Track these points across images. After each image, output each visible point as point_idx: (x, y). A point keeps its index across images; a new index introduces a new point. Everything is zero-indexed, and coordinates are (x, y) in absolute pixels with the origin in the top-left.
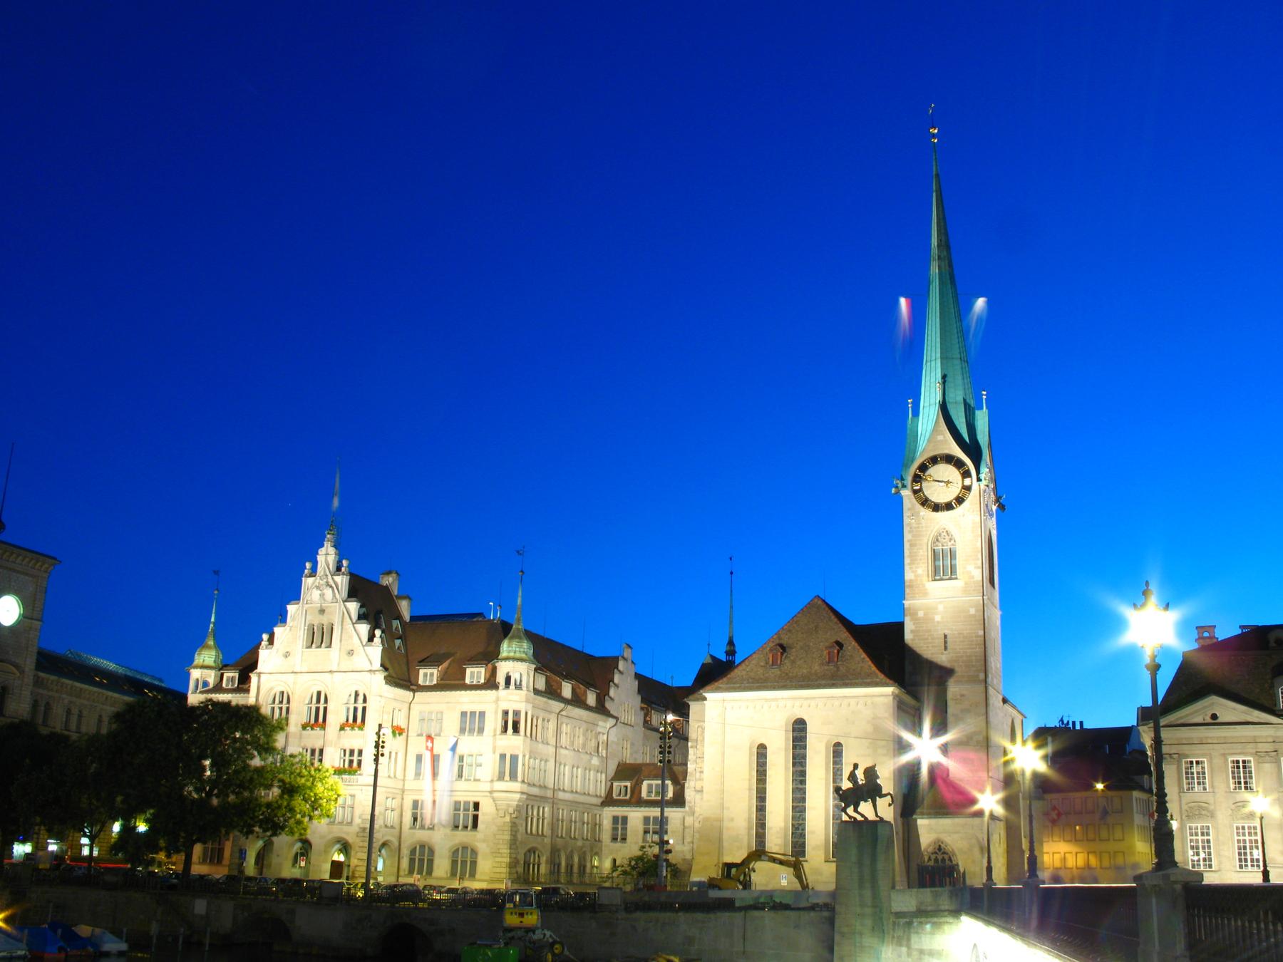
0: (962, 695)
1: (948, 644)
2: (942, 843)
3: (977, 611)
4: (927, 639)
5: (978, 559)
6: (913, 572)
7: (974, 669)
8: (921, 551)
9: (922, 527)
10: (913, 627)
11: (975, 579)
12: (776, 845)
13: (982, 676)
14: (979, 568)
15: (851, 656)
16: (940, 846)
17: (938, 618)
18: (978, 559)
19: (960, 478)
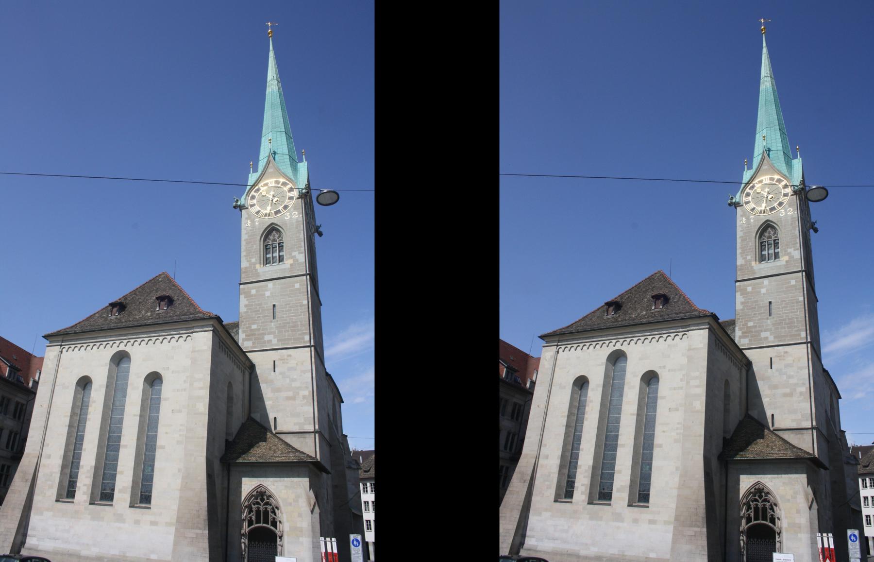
0: (786, 352)
4: (755, 308)
5: (797, 243)
7: (796, 329)
8: (750, 243)
9: (751, 226)
11: (795, 258)
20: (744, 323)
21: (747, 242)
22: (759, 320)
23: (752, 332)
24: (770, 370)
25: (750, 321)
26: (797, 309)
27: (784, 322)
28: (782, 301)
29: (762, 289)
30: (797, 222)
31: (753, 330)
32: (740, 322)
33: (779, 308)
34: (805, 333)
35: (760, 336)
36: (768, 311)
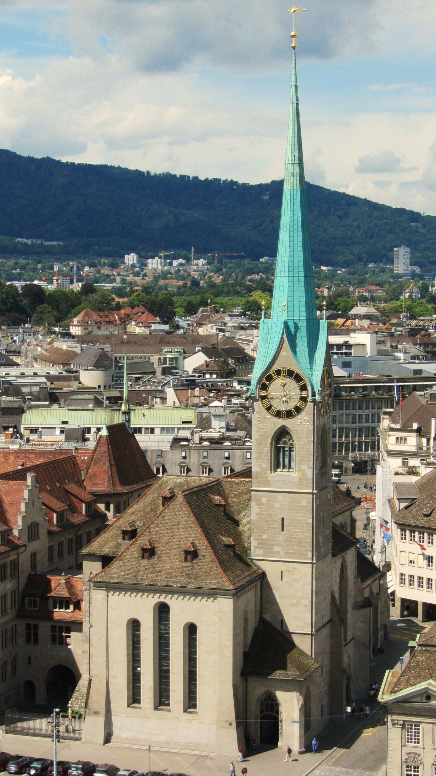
0: (294, 568)
1: (285, 527)
2: (271, 694)
3: (307, 502)
4: (269, 521)
6: (259, 465)
7: (304, 549)
9: (267, 429)
10: (258, 511)
11: (308, 477)
12: (148, 698)
13: (310, 554)
14: (310, 468)
15: (204, 556)
16: (270, 695)
17: (277, 505)
18: (310, 461)
19: (299, 391)
20: (259, 534)
21: (263, 447)
22: (272, 534)
23: (265, 544)
24: (280, 582)
25: (265, 533)
26: (306, 530)
27: (294, 540)
28: (293, 520)
29: (276, 503)
30: (312, 436)
31: (267, 543)
32: (257, 533)
33: (290, 526)
34: (311, 553)
35: (273, 549)
36: (281, 527)
